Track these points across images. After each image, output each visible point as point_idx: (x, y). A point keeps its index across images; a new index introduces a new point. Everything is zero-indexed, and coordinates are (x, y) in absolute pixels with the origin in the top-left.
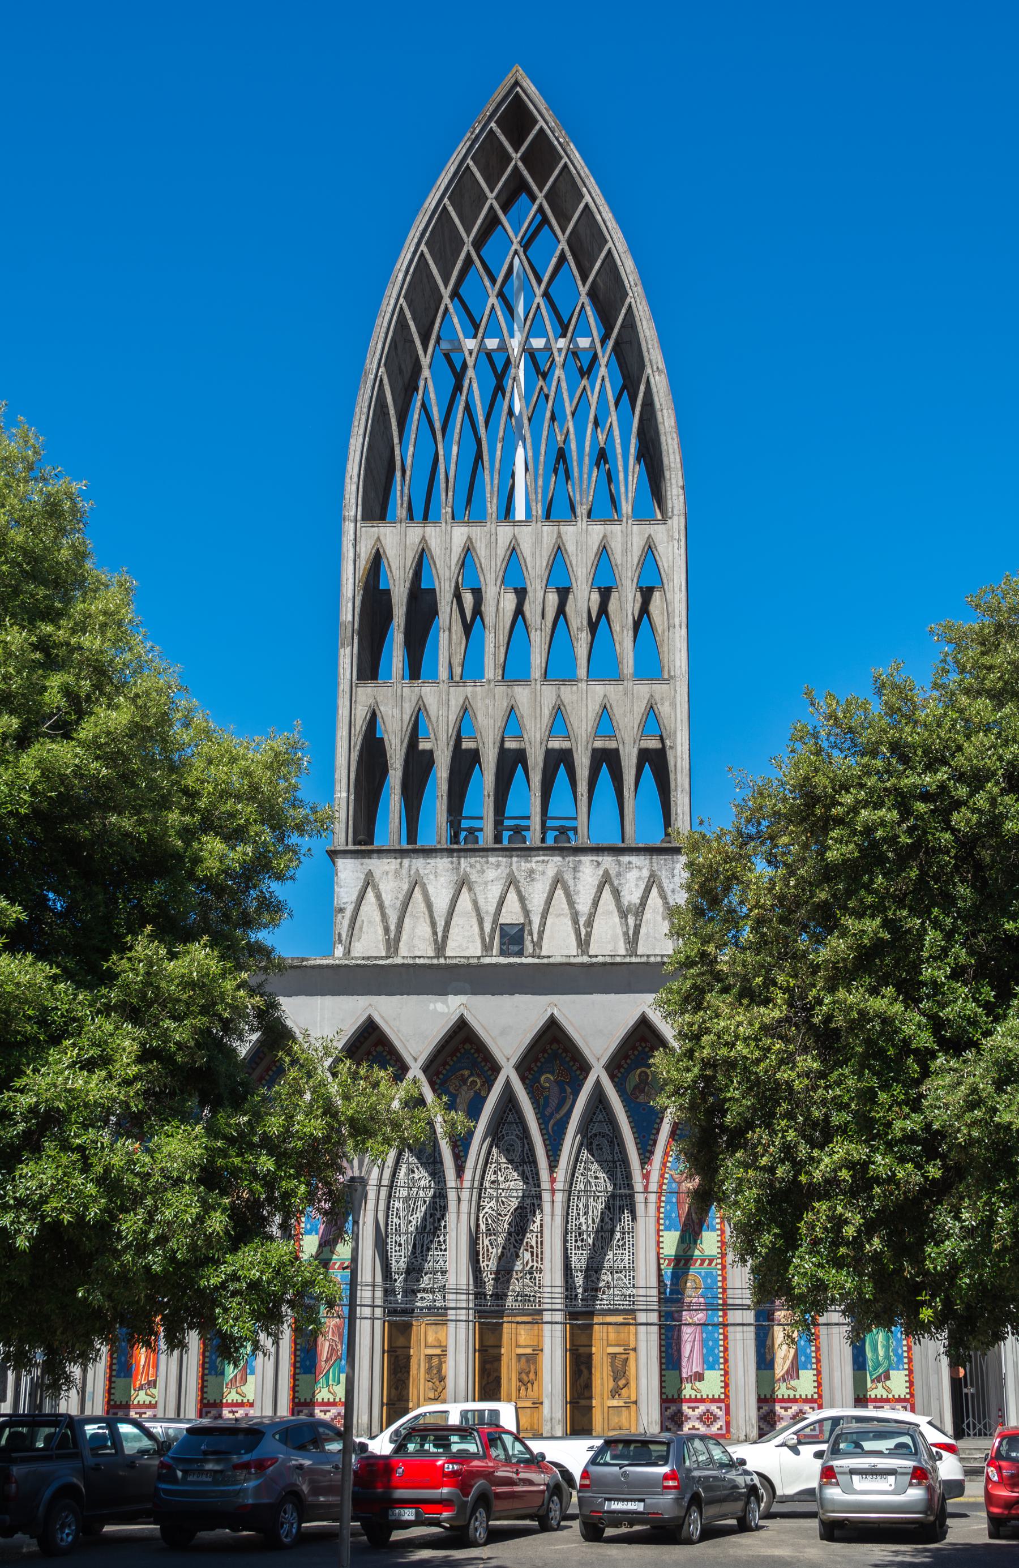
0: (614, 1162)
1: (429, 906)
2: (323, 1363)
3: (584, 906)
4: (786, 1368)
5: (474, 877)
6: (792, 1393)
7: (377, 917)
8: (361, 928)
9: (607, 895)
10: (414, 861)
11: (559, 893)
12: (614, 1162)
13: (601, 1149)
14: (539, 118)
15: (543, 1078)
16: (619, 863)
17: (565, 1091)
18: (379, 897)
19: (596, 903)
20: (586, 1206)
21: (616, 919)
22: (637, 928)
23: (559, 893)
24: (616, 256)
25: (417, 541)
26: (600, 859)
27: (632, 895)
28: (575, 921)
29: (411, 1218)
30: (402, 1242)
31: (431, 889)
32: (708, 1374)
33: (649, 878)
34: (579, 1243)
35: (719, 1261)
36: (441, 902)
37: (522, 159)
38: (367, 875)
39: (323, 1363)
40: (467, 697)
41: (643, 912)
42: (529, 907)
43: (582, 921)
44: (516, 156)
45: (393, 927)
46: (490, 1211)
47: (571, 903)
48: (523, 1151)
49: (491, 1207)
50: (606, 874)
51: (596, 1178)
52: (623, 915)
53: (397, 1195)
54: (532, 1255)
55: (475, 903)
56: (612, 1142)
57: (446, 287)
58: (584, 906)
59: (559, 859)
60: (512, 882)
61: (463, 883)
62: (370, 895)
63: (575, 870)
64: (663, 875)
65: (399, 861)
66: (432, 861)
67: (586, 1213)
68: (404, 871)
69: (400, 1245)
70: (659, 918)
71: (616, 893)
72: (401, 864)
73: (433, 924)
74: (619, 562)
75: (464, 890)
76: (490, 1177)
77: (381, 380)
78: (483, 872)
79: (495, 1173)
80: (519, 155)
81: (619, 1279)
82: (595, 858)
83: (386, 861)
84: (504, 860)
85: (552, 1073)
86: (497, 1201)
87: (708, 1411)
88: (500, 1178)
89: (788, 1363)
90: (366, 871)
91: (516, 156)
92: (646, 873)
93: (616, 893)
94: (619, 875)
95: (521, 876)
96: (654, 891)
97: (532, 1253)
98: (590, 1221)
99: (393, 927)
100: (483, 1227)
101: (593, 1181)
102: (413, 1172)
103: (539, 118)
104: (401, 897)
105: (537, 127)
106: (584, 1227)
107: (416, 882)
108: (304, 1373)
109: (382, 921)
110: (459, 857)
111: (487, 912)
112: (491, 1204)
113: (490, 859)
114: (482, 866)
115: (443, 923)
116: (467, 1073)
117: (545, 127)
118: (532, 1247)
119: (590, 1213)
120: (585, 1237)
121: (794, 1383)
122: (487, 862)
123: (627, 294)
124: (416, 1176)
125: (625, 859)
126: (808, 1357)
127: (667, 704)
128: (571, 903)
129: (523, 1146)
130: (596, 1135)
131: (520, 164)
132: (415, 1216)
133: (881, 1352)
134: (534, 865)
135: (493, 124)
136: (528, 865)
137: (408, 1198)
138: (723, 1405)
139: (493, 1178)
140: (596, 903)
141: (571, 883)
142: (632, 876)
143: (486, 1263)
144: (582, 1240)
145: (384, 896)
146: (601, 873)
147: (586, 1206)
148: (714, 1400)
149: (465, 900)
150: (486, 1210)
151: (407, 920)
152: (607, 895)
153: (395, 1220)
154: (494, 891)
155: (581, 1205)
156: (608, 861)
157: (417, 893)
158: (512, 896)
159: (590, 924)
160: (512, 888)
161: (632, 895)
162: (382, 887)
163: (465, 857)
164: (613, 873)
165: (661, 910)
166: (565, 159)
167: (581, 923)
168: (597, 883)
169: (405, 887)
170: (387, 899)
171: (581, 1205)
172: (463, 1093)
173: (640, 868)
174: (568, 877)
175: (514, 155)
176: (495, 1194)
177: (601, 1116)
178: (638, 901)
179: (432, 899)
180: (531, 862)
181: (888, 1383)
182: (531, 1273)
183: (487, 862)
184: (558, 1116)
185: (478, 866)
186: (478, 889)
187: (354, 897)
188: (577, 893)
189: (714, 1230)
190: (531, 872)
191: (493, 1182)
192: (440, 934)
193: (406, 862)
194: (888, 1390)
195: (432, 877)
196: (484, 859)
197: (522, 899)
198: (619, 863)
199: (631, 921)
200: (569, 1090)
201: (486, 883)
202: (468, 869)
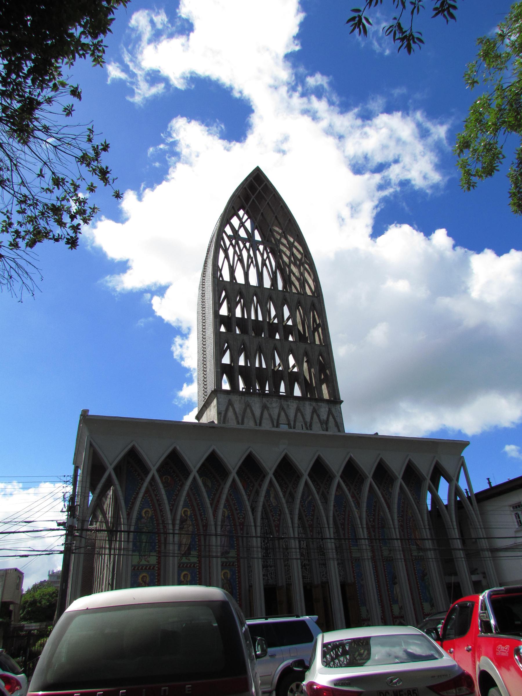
1: (253, 414)
5: (269, 405)
7: (234, 418)
11: (299, 414)
16: (318, 405)
18: (234, 410)
19: (312, 418)
21: (319, 425)
31: (253, 409)
36: (258, 413)
40: (259, 342)
43: (308, 425)
47: (304, 418)
50: (314, 408)
55: (270, 415)
59: (297, 401)
60: (282, 408)
61: (264, 407)
62: (231, 409)
64: (333, 410)
71: (318, 416)
72: (241, 398)
75: (265, 410)
92: (327, 409)
93: (318, 416)
95: (285, 407)
105: (265, 183)
107: (248, 405)
110: (263, 398)
115: (259, 421)
125: (320, 404)
128: (304, 418)
134: (289, 403)
136: (287, 403)
141: (303, 411)
143: (287, 562)
145: (236, 409)
146: (312, 408)
152: (315, 416)
157: (248, 410)
158: (283, 414)
162: (235, 406)
164: (316, 408)
165: (334, 423)
168: (311, 411)
169: (244, 407)
170: (237, 410)
174: (302, 408)
178: (326, 419)
180: (288, 402)
193: (243, 397)
195: (253, 404)
197: (287, 415)
198: (318, 405)
202: (266, 402)
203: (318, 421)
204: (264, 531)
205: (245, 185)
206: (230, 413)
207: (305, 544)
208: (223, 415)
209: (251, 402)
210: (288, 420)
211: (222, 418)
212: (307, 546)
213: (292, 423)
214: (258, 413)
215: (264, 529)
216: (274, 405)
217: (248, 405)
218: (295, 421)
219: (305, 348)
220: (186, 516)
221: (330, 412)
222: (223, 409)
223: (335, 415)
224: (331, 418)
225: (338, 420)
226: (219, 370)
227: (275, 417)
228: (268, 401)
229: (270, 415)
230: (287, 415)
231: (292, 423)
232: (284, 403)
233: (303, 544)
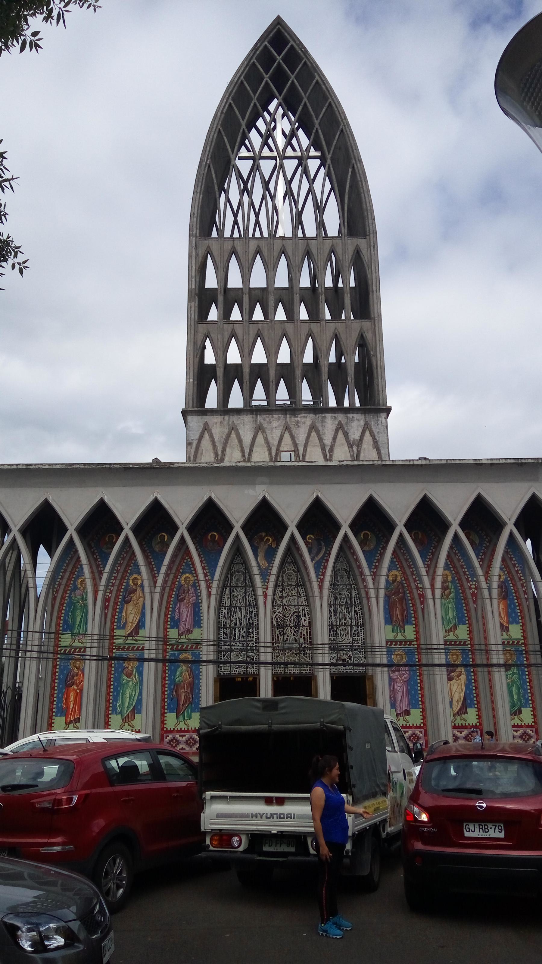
0: (350, 585)
1: (240, 441)
2: (181, 706)
3: (328, 441)
4: (459, 707)
5: (265, 425)
6: (464, 723)
7: (210, 447)
8: (202, 454)
9: (340, 435)
10: (231, 416)
11: (314, 434)
12: (350, 585)
13: (343, 578)
14: (291, 40)
15: (307, 537)
17: (321, 545)
18: (211, 436)
19: (334, 439)
20: (335, 611)
22: (358, 453)
23: (314, 434)
24: (334, 105)
25: (230, 247)
26: (336, 415)
27: (355, 435)
28: (323, 449)
29: (232, 619)
30: (228, 633)
31: (241, 432)
32: (412, 711)
33: (365, 425)
34: (332, 633)
35: (415, 643)
36: (247, 439)
37: (282, 59)
38: (205, 424)
39: (181, 706)
40: (259, 329)
41: (361, 444)
42: (297, 442)
44: (279, 58)
45: (220, 453)
46: (279, 614)
47: (321, 439)
48: (297, 579)
49: (279, 612)
50: (340, 423)
51: (340, 594)
52: (350, 445)
53: (224, 605)
54: (304, 640)
56: (349, 574)
57: (243, 120)
58: (328, 441)
59: (312, 416)
60: (287, 428)
61: (259, 429)
62: (206, 436)
63: (322, 421)
64: (373, 424)
65: (223, 417)
66: (242, 417)
67: (335, 615)
68: (226, 422)
69: (226, 634)
70: (371, 448)
71: (346, 434)
72: (224, 418)
73: (243, 451)
74: (341, 258)
75: (260, 433)
76: (279, 594)
77: (209, 166)
78: (270, 423)
79: (281, 592)
80: (281, 57)
81: (357, 654)
82: (333, 415)
83: (215, 417)
84: (282, 416)
85: (313, 534)
86: (283, 608)
87: (414, 734)
88: (284, 595)
89: (460, 704)
90: (204, 422)
91: (279, 58)
92: (362, 423)
93: (346, 434)
94: (347, 424)
96: (367, 433)
97: (304, 639)
98: (338, 620)
99: (220, 453)
100: (275, 623)
101: (338, 596)
102: (233, 591)
103: (291, 40)
104: (224, 436)
105: (290, 44)
106: (334, 623)
107: (233, 428)
108: (170, 712)
109: (214, 449)
110: (257, 415)
111: (273, 445)
112: (279, 610)
113: (274, 415)
114: (270, 420)
115: (248, 451)
116: (264, 534)
117: (294, 44)
118: (304, 635)
119: (338, 615)
120: (335, 629)
121: (464, 716)
122: (272, 417)
123: (340, 124)
124: (235, 593)
125: (350, 415)
126: (472, 700)
127: (370, 332)
128: (321, 439)
129: (297, 577)
130: (339, 570)
131: (281, 61)
132: (235, 617)
133: (515, 697)
134: (299, 419)
135: (266, 43)
136: (296, 419)
137: (231, 606)
138: (422, 730)
139: (280, 594)
140: (334, 439)
141: (320, 428)
142: (354, 424)
144: (333, 631)
146: (337, 423)
147: (335, 611)
148: (417, 727)
149: (260, 438)
150: (276, 613)
151: (228, 450)
152: (340, 435)
153: (223, 620)
154: (277, 433)
155: (332, 611)
157: (233, 435)
158: (287, 436)
159: (331, 450)
160: (287, 432)
161: (355, 435)
162: (213, 431)
163: (260, 415)
165: (372, 443)
166: (305, 59)
167: (327, 451)
169: (226, 431)
170: (216, 437)
171: (332, 611)
172: (262, 545)
173: (358, 420)
174: (319, 425)
175: (278, 57)
176: (281, 604)
177: (341, 559)
178: (358, 438)
179: (242, 437)
180: (297, 417)
181: (521, 715)
182: (304, 651)
183: (272, 417)
184: (317, 559)
185: (267, 419)
186: (268, 432)
187: (197, 437)
188: (324, 434)
189: (412, 624)
190: (298, 422)
191: (280, 597)
192: (247, 457)
193: (227, 417)
194: (521, 720)
195: (241, 425)
196: (271, 416)
197: (293, 437)
199: (355, 449)
200: (323, 544)
201: (272, 429)
202: (262, 421)
203: (344, 441)
204: (246, 603)
205: (254, 58)
206: (206, 442)
207: (307, 621)
208: (194, 445)
209: (238, 422)
210: (295, 445)
211: (193, 451)
212: (309, 622)
213: (301, 449)
214: (247, 439)
215: (246, 599)
216: (275, 424)
217: (233, 428)
218: (305, 447)
219: (336, 329)
220: (136, 585)
221: (366, 427)
222: (195, 436)
223: (375, 430)
224: (367, 436)
225: (380, 438)
226: (191, 380)
227: (274, 442)
228: (264, 420)
230: (293, 437)
231: (301, 449)
232: (291, 420)
233: (305, 620)
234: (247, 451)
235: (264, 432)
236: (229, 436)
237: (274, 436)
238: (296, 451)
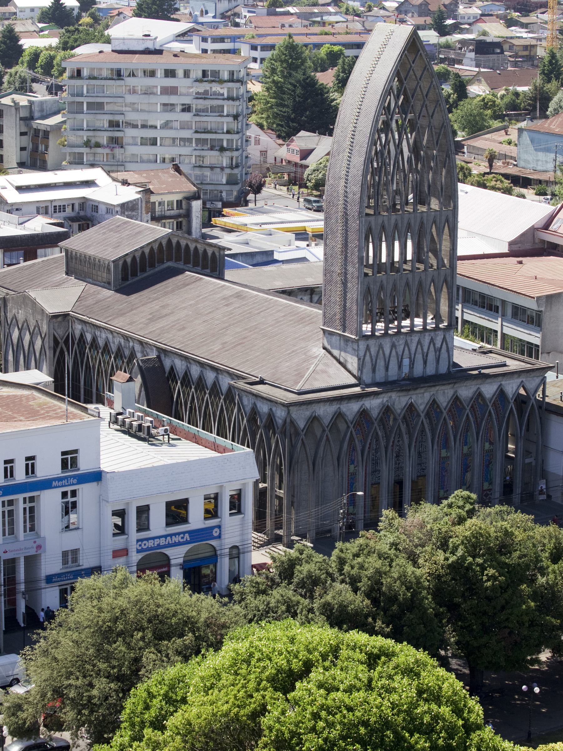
5: (397, 344)
22: (439, 355)
28: (423, 356)
47: (422, 349)
64: (447, 336)
93: (434, 345)
95: (409, 341)
107: (381, 347)
125: (437, 333)
154: (402, 347)
156: (432, 334)
158: (406, 349)
159: (427, 356)
170: (373, 353)
197: (409, 350)
206: (368, 358)
213: (413, 356)
216: (401, 342)
221: (444, 339)
223: (448, 340)
229: (397, 353)
230: (409, 350)
231: (413, 356)
232: (409, 338)
234: (387, 360)
235: (396, 348)
236: (378, 352)
237: (400, 349)
238: (410, 358)
